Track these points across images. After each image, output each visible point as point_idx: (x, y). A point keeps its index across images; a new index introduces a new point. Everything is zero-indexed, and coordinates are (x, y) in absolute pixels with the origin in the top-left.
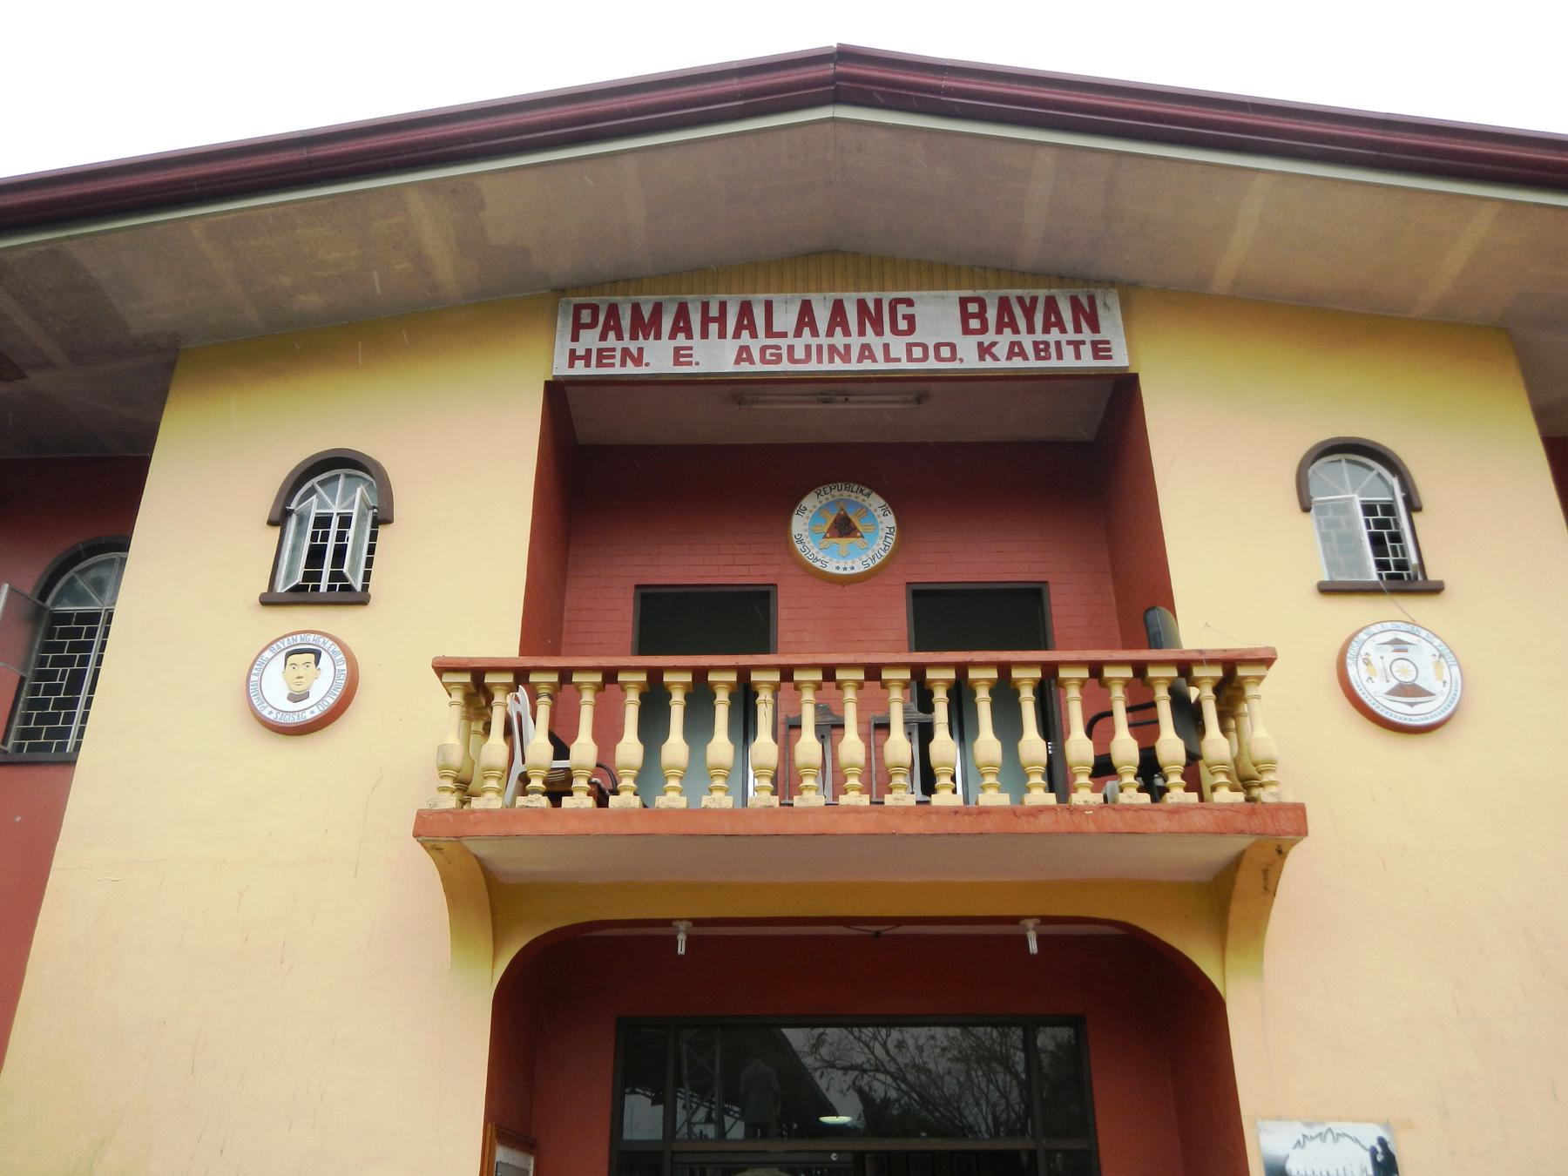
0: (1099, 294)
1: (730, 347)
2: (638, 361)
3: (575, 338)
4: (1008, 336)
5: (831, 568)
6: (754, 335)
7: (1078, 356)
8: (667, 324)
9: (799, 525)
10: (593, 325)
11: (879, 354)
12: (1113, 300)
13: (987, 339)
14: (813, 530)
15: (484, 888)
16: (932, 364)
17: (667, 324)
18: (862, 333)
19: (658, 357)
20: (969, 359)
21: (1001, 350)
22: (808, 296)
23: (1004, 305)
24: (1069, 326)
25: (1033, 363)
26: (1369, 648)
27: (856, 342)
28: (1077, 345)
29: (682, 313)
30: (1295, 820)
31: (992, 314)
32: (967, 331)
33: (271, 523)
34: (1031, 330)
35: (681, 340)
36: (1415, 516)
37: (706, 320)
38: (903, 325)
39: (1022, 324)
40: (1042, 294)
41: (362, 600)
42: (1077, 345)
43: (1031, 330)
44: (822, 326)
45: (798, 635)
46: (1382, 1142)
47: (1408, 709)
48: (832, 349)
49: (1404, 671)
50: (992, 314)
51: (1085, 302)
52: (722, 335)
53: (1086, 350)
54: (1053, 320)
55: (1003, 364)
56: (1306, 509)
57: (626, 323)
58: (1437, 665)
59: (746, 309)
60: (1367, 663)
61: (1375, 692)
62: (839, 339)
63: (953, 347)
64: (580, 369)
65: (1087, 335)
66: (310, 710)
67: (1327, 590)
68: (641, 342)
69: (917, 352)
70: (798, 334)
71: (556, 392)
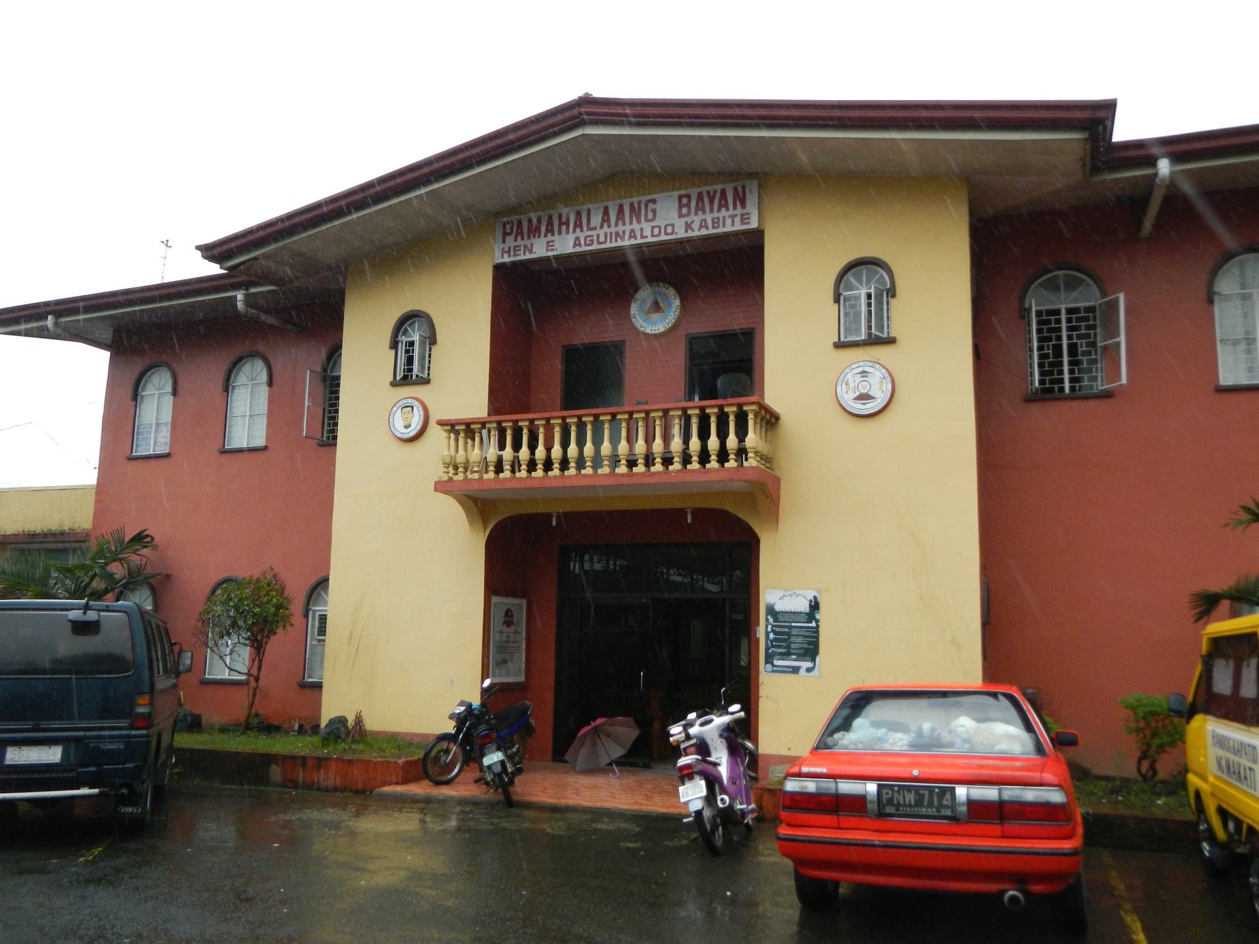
0: (747, 183)
1: (571, 239)
2: (531, 252)
3: (504, 242)
4: (700, 216)
5: (648, 331)
6: (582, 230)
7: (733, 224)
8: (543, 229)
9: (634, 309)
10: (510, 234)
11: (638, 235)
12: (755, 188)
13: (689, 219)
14: (641, 309)
15: (478, 504)
16: (663, 237)
17: (543, 229)
18: (631, 223)
19: (539, 249)
20: (681, 233)
21: (696, 226)
22: (606, 204)
23: (700, 197)
24: (731, 206)
25: (711, 231)
26: (849, 376)
27: (628, 228)
28: (733, 217)
29: (550, 223)
31: (693, 204)
32: (681, 216)
33: (391, 348)
34: (712, 211)
35: (550, 237)
36: (892, 301)
37: (561, 224)
38: (650, 216)
39: (707, 209)
40: (719, 187)
41: (427, 381)
42: (733, 217)
43: (712, 211)
44: (613, 221)
45: (634, 370)
46: (815, 598)
47: (862, 407)
48: (617, 234)
49: (864, 387)
50: (693, 204)
51: (740, 190)
52: (567, 232)
53: (737, 219)
54: (723, 204)
55: (696, 233)
56: (837, 300)
57: (525, 230)
58: (881, 383)
59: (578, 214)
60: (847, 384)
61: (848, 398)
62: (620, 228)
63: (673, 225)
64: (507, 259)
65: (739, 211)
66: (412, 432)
67: (839, 345)
68: (532, 240)
69: (656, 231)
70: (602, 227)
71: (499, 269)
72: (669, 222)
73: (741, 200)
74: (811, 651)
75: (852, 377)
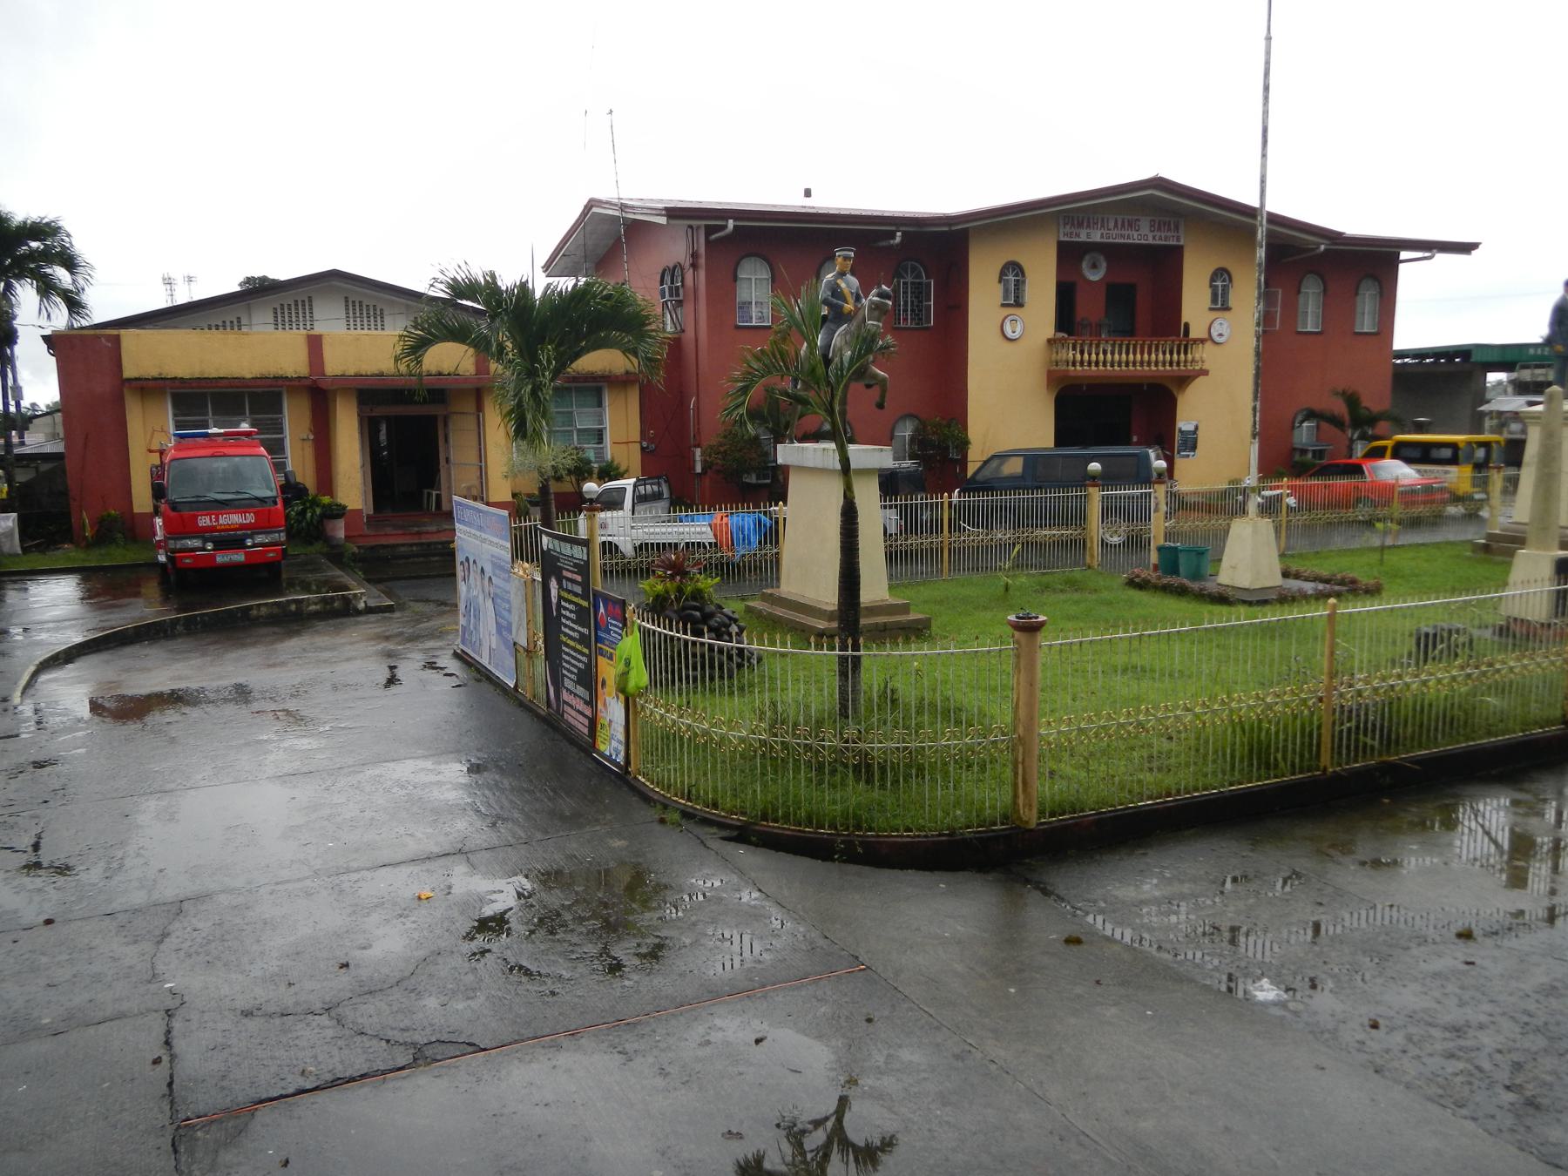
9: (1084, 265)
19: (1083, 238)
20: (1151, 241)
30: (1205, 373)
66: (1016, 335)
72: (1143, 234)
73: (1177, 228)
74: (1194, 448)
75: (1216, 324)
